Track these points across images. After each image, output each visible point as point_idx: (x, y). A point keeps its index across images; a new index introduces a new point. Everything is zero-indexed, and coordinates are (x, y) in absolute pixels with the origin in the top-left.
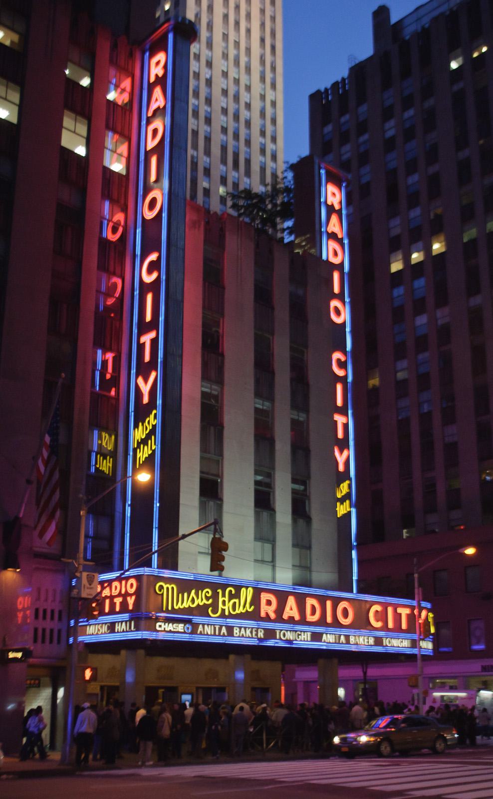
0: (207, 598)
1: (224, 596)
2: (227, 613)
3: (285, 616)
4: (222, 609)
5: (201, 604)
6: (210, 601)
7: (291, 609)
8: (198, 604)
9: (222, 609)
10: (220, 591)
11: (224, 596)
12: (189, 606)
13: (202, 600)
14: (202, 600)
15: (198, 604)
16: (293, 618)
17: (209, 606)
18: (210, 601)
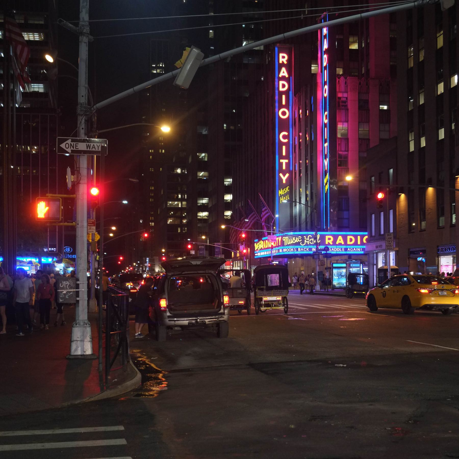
0: (300, 240)
2: (308, 244)
3: (337, 243)
4: (306, 242)
5: (297, 242)
6: (301, 240)
7: (340, 240)
8: (296, 242)
9: (306, 242)
10: (305, 237)
12: (293, 243)
13: (297, 240)
14: (297, 240)
15: (296, 242)
16: (341, 243)
17: (300, 242)
18: (301, 240)
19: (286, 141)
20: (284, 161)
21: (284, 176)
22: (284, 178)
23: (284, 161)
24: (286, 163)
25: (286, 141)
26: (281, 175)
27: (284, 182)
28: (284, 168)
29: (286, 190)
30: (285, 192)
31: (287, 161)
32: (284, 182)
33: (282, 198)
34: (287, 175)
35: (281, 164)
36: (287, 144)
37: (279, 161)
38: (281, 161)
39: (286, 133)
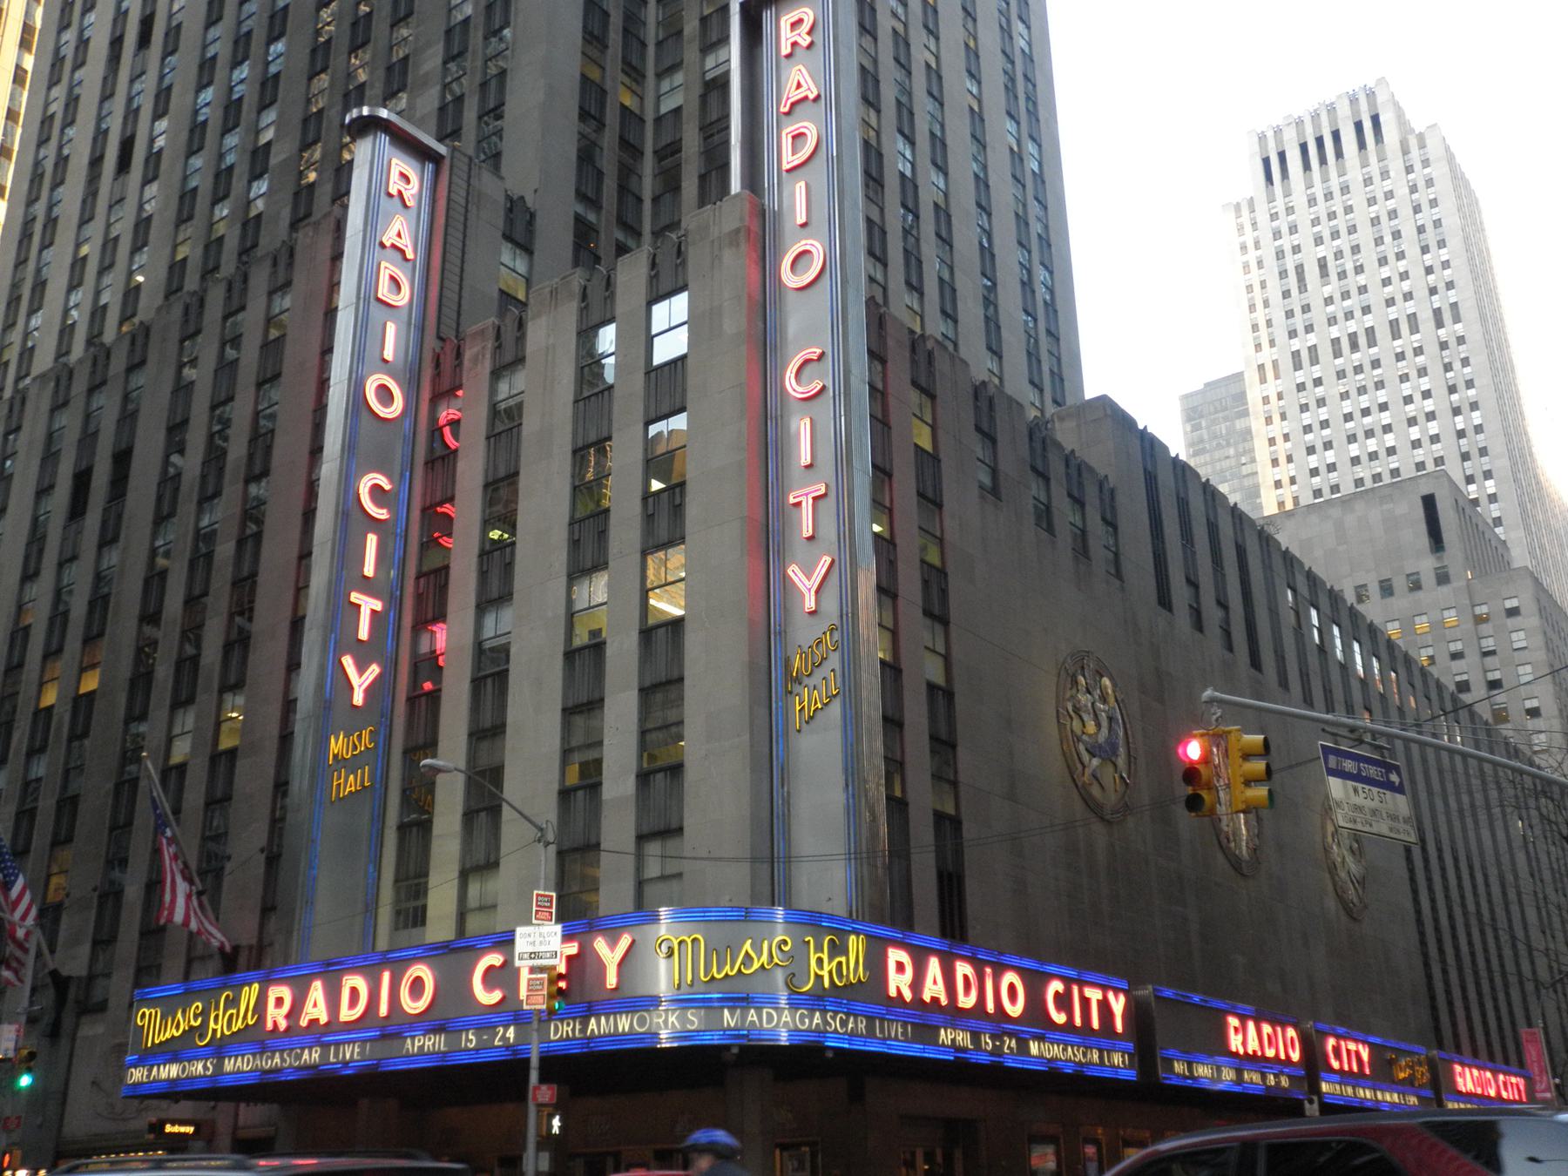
1: (819, 948)
11: (819, 948)
19: (381, 514)
20: (369, 605)
21: (361, 670)
22: (361, 681)
24: (373, 612)
25: (381, 514)
26: (348, 661)
27: (358, 699)
29: (360, 737)
30: (355, 748)
31: (378, 605)
33: (339, 778)
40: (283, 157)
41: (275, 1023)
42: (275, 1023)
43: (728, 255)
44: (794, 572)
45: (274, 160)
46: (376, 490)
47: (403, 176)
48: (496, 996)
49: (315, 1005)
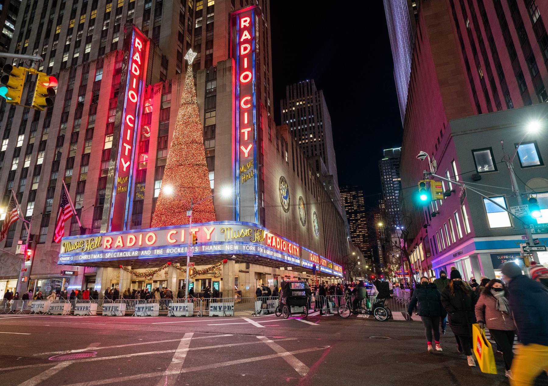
19: (131, 125)
23: (128, 147)
25: (131, 125)
26: (122, 160)
27: (125, 169)
28: (126, 154)
32: (125, 169)
34: (128, 163)
35: (124, 148)
36: (132, 129)
37: (123, 144)
38: (125, 144)
39: (133, 119)
40: (95, 39)
41: (106, 246)
42: (106, 246)
43: (228, 73)
44: (243, 148)
45: (93, 40)
46: (130, 119)
47: (138, 43)
48: (175, 241)
49: (119, 242)
